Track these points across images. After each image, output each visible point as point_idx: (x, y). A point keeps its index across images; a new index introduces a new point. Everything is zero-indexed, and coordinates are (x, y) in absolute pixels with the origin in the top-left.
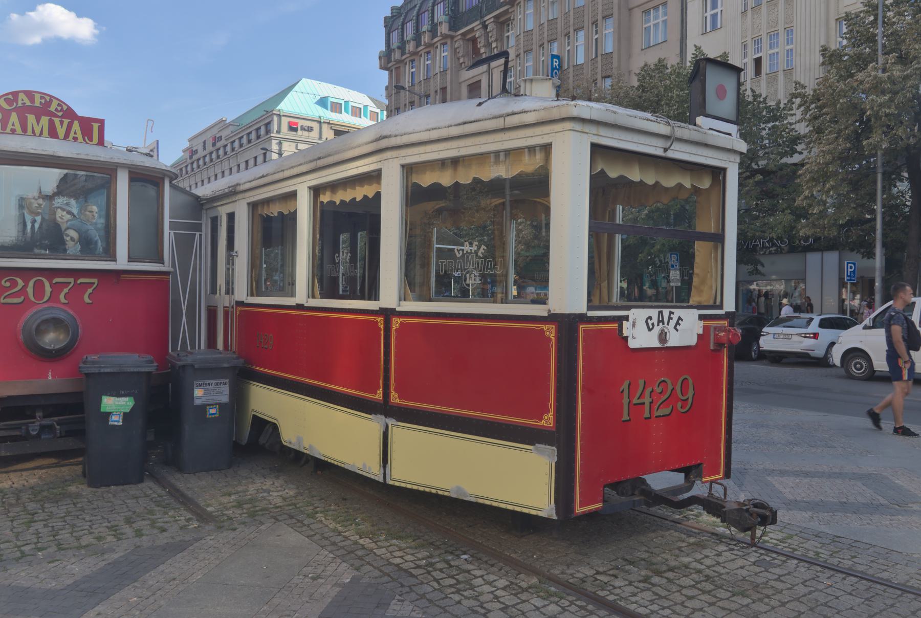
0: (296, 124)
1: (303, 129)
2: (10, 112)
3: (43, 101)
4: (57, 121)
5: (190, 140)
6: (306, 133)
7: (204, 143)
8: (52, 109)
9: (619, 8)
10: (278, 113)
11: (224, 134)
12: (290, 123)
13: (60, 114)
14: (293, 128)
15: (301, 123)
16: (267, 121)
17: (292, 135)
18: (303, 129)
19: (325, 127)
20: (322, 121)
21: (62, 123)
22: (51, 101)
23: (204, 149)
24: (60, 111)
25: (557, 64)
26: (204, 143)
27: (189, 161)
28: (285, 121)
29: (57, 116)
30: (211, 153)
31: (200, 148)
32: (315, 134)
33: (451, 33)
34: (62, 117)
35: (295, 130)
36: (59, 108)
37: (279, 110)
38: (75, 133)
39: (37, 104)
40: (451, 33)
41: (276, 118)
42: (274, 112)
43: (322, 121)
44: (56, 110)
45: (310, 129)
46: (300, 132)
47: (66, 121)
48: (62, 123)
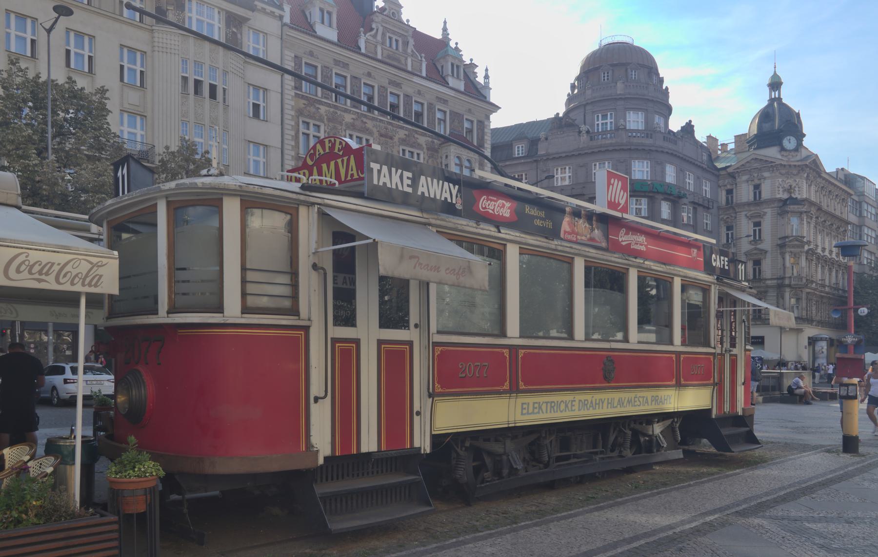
2: (313, 165)
3: (330, 145)
4: (339, 161)
8: (336, 150)
13: (341, 153)
21: (343, 161)
22: (335, 140)
24: (341, 150)
29: (339, 156)
34: (343, 156)
36: (340, 147)
38: (352, 170)
39: (327, 150)
44: (339, 150)
47: (345, 159)
48: (343, 161)
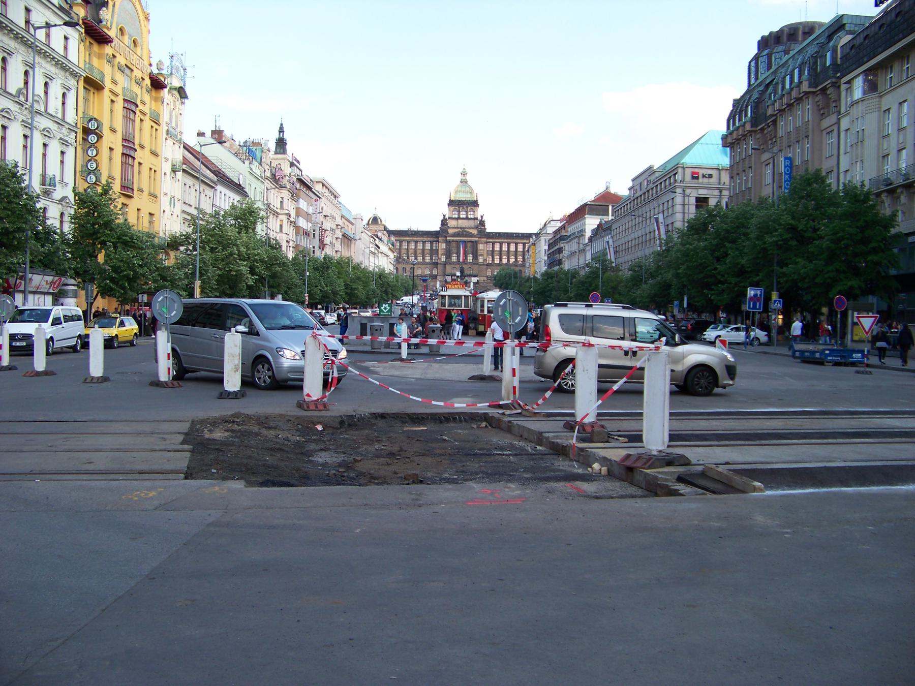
0: (697, 173)
1: (704, 176)
5: (633, 180)
6: (706, 180)
7: (641, 184)
9: (813, 131)
10: (682, 166)
11: (652, 178)
12: (693, 173)
14: (695, 177)
15: (701, 172)
16: (675, 172)
17: (694, 183)
18: (704, 176)
19: (723, 173)
20: (721, 168)
23: (641, 190)
25: (788, 163)
26: (641, 184)
27: (632, 199)
28: (688, 172)
30: (645, 193)
31: (638, 188)
32: (714, 180)
33: (753, 129)
35: (697, 178)
37: (683, 164)
40: (753, 129)
41: (680, 170)
42: (679, 166)
43: (721, 168)
45: (710, 176)
46: (701, 179)
